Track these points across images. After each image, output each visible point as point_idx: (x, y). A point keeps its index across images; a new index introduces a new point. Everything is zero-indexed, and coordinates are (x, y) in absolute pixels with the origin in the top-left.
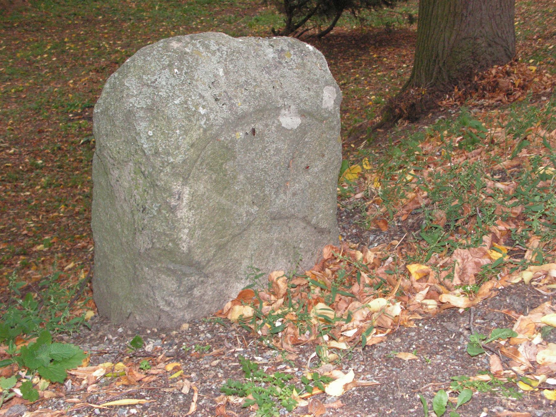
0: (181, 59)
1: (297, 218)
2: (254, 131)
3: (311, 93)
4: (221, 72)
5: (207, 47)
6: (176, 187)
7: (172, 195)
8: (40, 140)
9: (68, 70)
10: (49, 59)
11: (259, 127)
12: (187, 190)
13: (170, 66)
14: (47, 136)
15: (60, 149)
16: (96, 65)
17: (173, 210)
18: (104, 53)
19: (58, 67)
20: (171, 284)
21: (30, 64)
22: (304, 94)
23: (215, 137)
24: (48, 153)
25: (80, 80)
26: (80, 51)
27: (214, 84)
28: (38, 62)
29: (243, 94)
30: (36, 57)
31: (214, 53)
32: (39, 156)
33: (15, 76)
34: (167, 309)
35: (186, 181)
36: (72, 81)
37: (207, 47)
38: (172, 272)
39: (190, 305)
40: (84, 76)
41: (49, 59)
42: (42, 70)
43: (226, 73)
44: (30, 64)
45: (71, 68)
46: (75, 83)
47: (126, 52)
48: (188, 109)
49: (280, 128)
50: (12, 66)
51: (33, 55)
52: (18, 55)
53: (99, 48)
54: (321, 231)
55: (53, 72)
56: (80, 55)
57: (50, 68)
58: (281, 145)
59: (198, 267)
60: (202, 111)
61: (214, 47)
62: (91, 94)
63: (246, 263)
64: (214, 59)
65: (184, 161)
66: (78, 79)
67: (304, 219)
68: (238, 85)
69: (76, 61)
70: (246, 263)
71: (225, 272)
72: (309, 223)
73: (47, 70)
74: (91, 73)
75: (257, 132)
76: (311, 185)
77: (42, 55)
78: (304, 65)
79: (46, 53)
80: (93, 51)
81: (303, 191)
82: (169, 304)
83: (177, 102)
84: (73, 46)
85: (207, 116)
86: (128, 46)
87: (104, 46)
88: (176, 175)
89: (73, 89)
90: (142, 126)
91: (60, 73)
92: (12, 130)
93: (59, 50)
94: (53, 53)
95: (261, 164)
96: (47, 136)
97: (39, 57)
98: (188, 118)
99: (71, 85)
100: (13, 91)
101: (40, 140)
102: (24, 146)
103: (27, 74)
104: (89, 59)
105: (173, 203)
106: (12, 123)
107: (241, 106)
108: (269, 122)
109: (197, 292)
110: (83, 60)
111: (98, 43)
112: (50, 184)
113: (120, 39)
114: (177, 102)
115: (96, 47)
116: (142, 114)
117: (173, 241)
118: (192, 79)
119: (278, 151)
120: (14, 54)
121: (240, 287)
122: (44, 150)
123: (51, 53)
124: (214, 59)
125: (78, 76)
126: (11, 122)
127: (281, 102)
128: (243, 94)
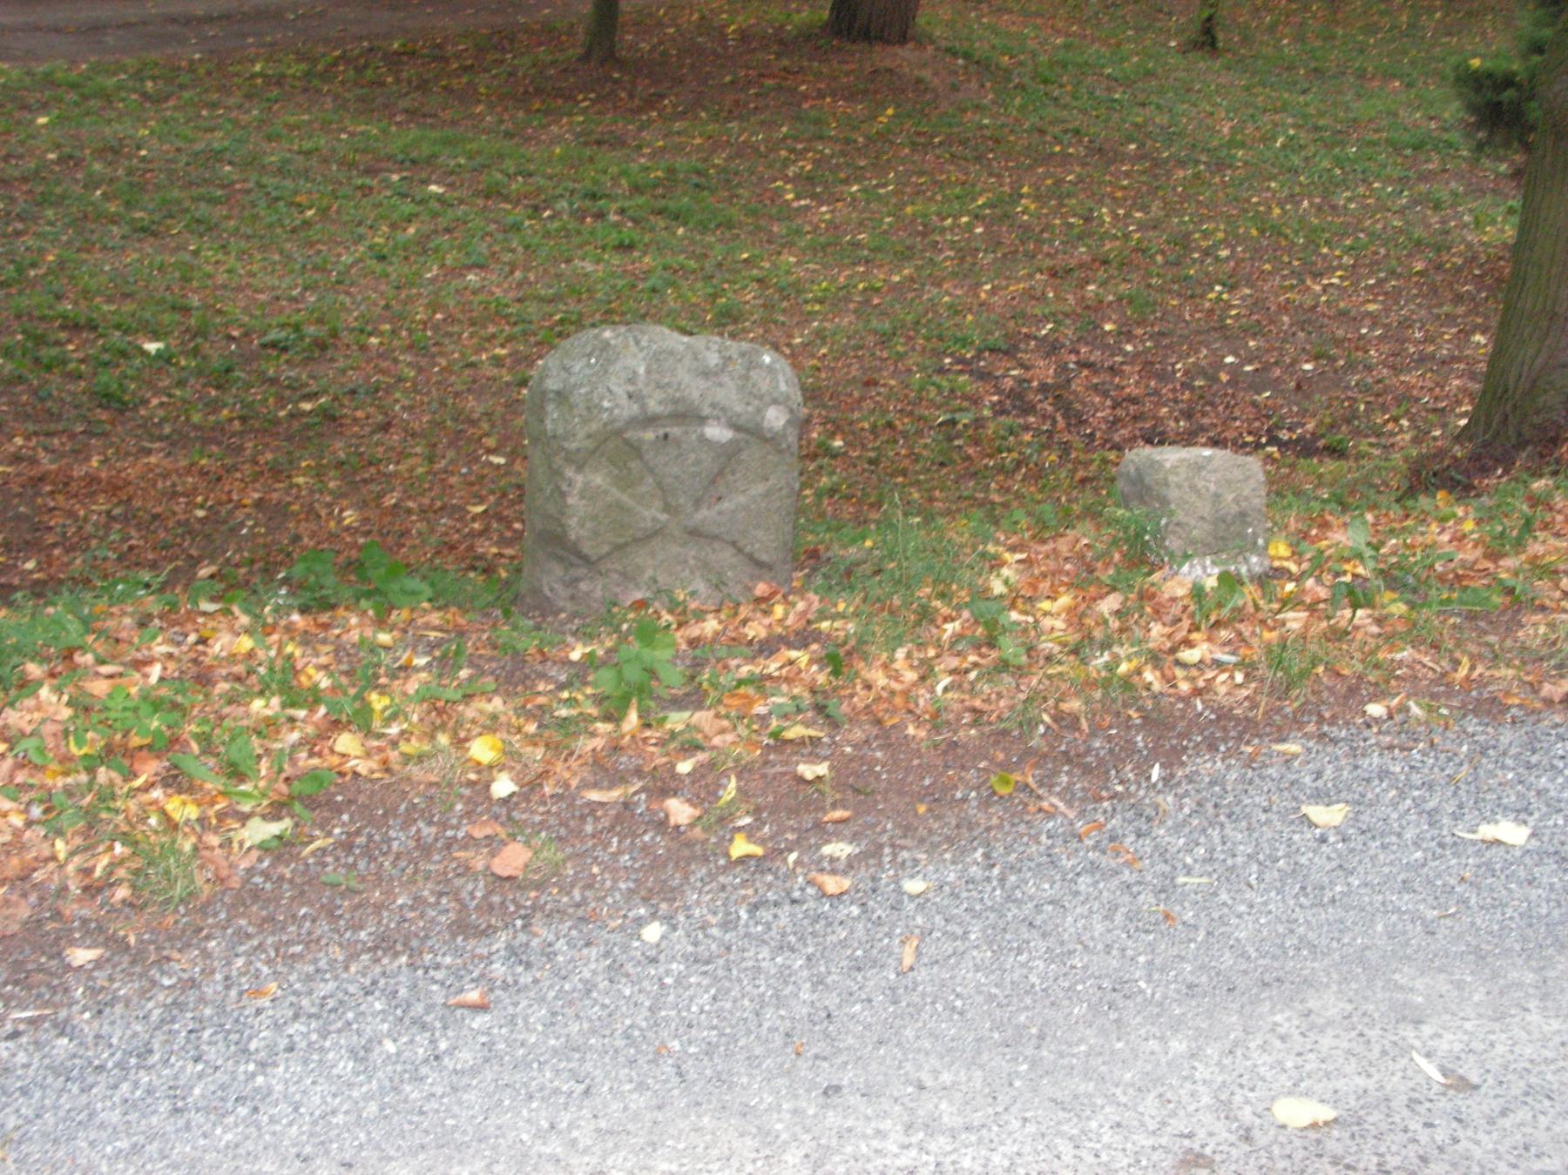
0: (602, 350)
1: (723, 541)
2: (666, 436)
3: (750, 409)
4: (642, 370)
5: (637, 342)
6: (569, 472)
7: (564, 479)
8: (862, 399)
9: (995, 259)
10: (969, 227)
11: (676, 431)
12: (579, 480)
13: (590, 355)
14: (879, 394)
15: (890, 425)
16: (1060, 262)
17: (563, 495)
18: (1090, 235)
19: (977, 250)
20: (558, 570)
21: (924, 235)
22: (739, 408)
23: (619, 433)
24: (862, 429)
25: (1007, 287)
26: (1044, 221)
27: (631, 380)
28: (943, 231)
29: (659, 395)
30: (944, 219)
31: (642, 350)
32: (843, 432)
33: (880, 256)
34: (548, 593)
35: (580, 468)
36: (988, 287)
37: (637, 342)
38: (561, 560)
39: (572, 598)
40: (1019, 281)
41: (969, 227)
42: (941, 251)
43: (648, 372)
44: (924, 235)
45: (1005, 255)
46: (993, 292)
47: (1139, 241)
48: (590, 400)
49: (703, 440)
50: (885, 232)
51: (938, 215)
52: (909, 210)
53: (1087, 220)
54: (760, 564)
55: (962, 259)
56: (1037, 229)
57: (960, 250)
58: (703, 456)
59: (585, 559)
60: (606, 404)
61: (644, 343)
62: (1012, 324)
63: (649, 573)
64: (641, 355)
65: (578, 450)
66: (1004, 283)
67: (734, 544)
68: (659, 386)
69: (1023, 243)
70: (649, 573)
71: (624, 574)
72: (740, 551)
73: (952, 253)
74: (1038, 276)
75: (671, 437)
76: (746, 508)
77: (956, 217)
78: (746, 378)
79: (968, 213)
80: (1071, 226)
81: (733, 512)
82: (552, 590)
83: (583, 391)
84: (1033, 207)
85: (610, 410)
86: (1155, 228)
87: (1100, 216)
88: (569, 460)
89: (982, 304)
90: (550, 407)
91: (974, 264)
92: (819, 369)
93: (998, 211)
94: (984, 217)
95: (676, 470)
96: (879, 394)
97: (950, 221)
98: (588, 408)
99: (983, 295)
100: (861, 286)
101: (862, 399)
102: (824, 406)
103: (905, 255)
104: (1051, 241)
105: (564, 488)
106: (824, 355)
107: (654, 406)
108: (691, 429)
109: (583, 586)
110: (1039, 242)
111: (1091, 210)
112: (832, 491)
113: (1145, 208)
114: (583, 391)
115: (1081, 217)
116: (551, 395)
117: (562, 526)
118: (606, 372)
119: (698, 462)
120: (901, 206)
121: (639, 595)
122: (859, 420)
123: (977, 217)
124: (641, 355)
125: (1008, 278)
126: (824, 351)
127: (706, 411)
128: (659, 395)
